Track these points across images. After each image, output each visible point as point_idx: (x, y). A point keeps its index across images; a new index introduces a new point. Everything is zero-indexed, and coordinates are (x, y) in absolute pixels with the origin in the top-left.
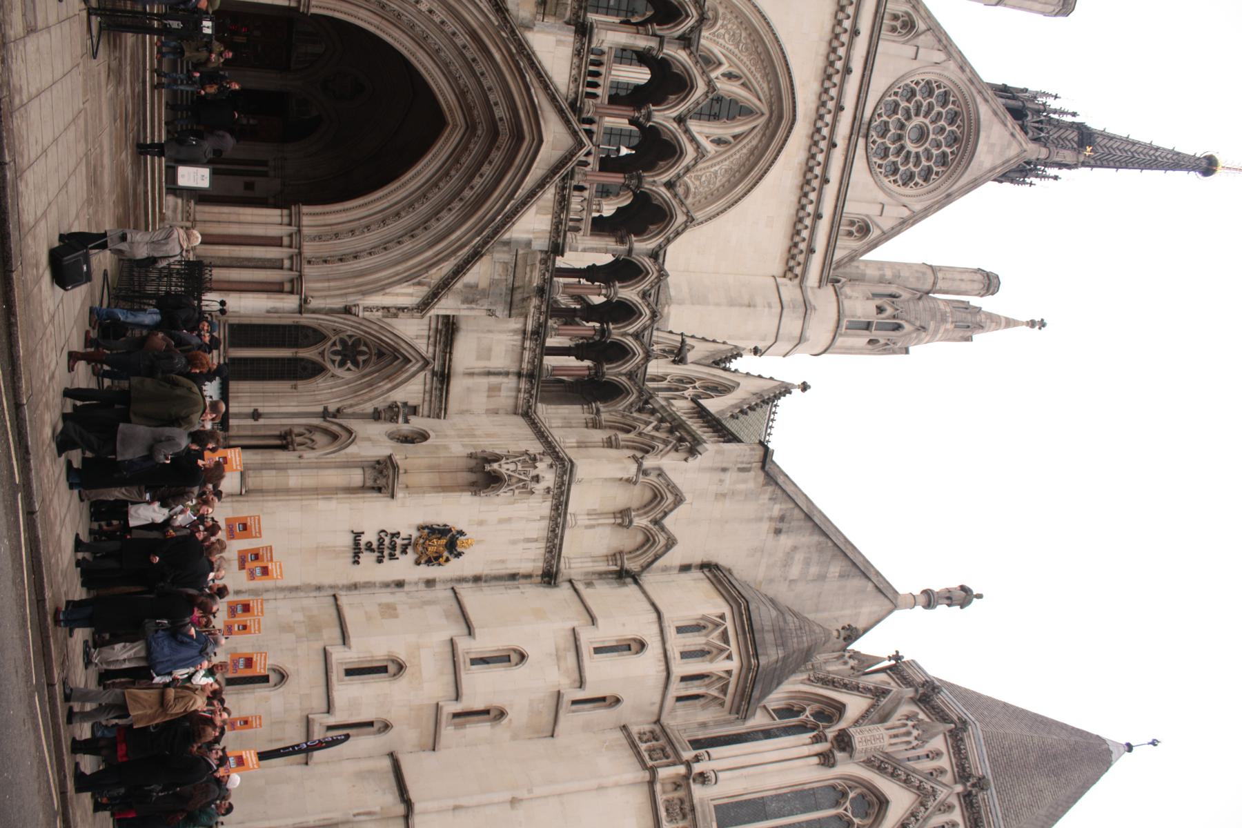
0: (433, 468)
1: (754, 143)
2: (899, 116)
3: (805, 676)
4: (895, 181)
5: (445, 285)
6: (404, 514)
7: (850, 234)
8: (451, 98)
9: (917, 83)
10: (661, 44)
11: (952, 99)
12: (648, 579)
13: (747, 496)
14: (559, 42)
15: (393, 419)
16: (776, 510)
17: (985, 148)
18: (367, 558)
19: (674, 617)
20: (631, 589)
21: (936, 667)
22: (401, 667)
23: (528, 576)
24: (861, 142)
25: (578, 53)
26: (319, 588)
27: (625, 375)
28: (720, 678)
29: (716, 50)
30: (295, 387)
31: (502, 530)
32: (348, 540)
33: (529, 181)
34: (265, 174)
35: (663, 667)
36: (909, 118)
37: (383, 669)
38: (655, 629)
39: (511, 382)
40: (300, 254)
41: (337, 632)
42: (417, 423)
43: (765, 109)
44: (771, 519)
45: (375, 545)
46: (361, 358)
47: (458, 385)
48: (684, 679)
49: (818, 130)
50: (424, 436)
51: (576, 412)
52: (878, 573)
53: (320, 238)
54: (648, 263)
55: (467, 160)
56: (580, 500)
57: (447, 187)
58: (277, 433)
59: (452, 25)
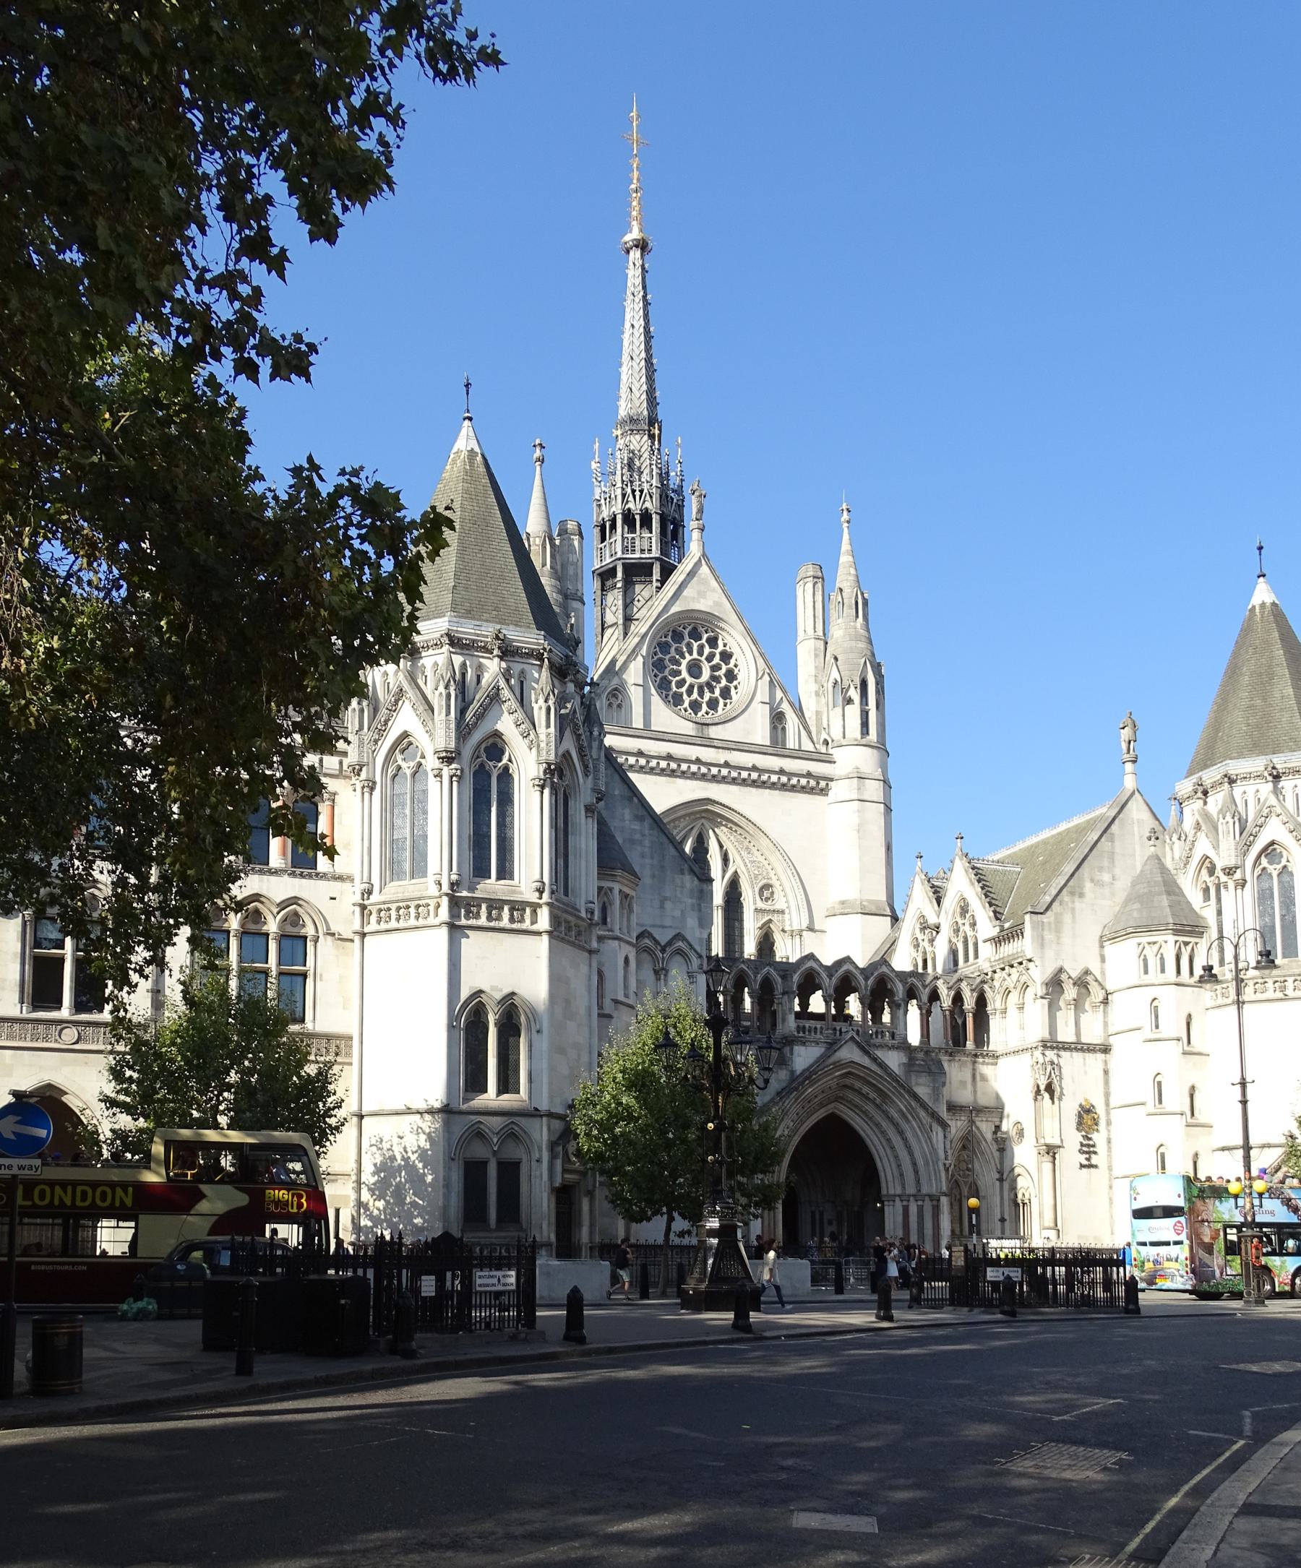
5: (934, 1116)
6: (1073, 1139)
18: (1093, 1162)
25: (804, 1044)
33: (874, 1067)
51: (995, 1024)
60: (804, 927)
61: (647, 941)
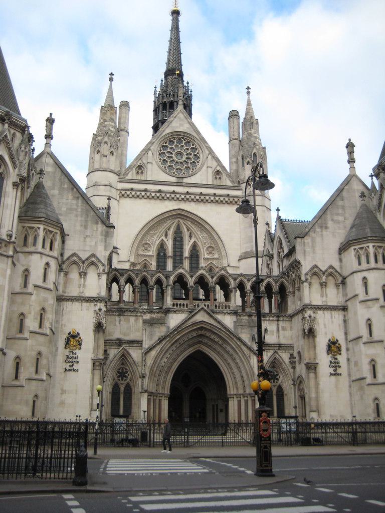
0: (309, 351)
1: (190, 223)
2: (173, 165)
3: (378, 213)
4: (198, 162)
6: (324, 360)
7: (220, 178)
8: (191, 349)
9: (160, 159)
10: (170, 285)
11: (164, 144)
12: (345, 274)
13: (313, 241)
14: (172, 319)
15: (294, 362)
16: (318, 230)
17: (181, 128)
18: (339, 371)
19: (355, 266)
20: (348, 280)
21: (375, 161)
22: (373, 360)
23: (345, 316)
24: (185, 180)
25: (175, 312)
26: (350, 386)
27: (276, 284)
28: (376, 249)
29: (158, 242)
30: (286, 395)
31: (328, 326)
32: (333, 378)
34: (217, 405)
35: (371, 271)
36: (174, 160)
37: (374, 366)
38: (359, 274)
39: (281, 324)
40: (242, 394)
41: (362, 381)
42: (296, 355)
43: (177, 220)
44: (322, 231)
45: (334, 368)
46: (275, 373)
47: (283, 341)
48: (376, 262)
49: (183, 199)
50: (299, 353)
51: (290, 300)
52: (342, 185)
53: (237, 388)
54: (238, 281)
55: (210, 343)
56: (317, 301)
57: (219, 349)
58: (300, 400)
59: (170, 351)
60: (227, 266)
61: (75, 258)
